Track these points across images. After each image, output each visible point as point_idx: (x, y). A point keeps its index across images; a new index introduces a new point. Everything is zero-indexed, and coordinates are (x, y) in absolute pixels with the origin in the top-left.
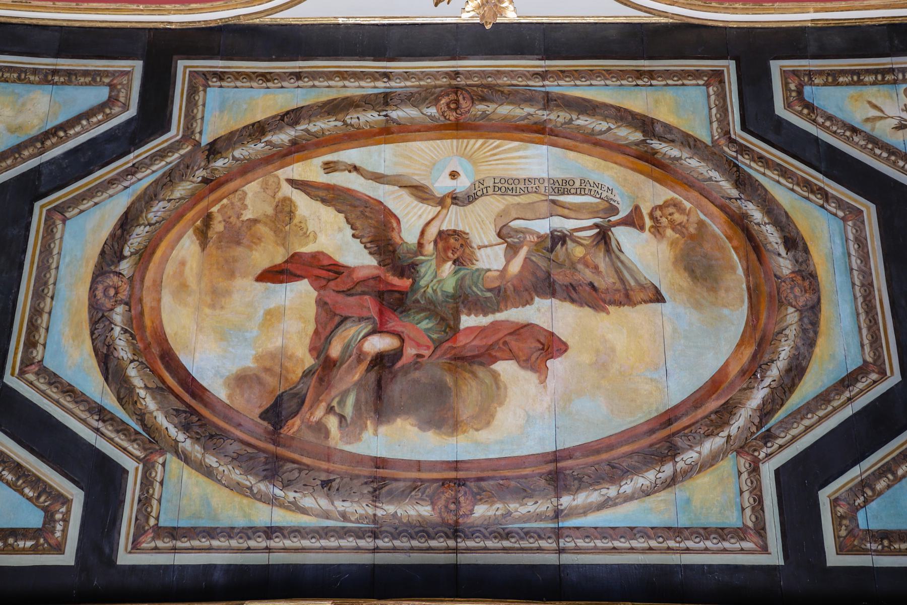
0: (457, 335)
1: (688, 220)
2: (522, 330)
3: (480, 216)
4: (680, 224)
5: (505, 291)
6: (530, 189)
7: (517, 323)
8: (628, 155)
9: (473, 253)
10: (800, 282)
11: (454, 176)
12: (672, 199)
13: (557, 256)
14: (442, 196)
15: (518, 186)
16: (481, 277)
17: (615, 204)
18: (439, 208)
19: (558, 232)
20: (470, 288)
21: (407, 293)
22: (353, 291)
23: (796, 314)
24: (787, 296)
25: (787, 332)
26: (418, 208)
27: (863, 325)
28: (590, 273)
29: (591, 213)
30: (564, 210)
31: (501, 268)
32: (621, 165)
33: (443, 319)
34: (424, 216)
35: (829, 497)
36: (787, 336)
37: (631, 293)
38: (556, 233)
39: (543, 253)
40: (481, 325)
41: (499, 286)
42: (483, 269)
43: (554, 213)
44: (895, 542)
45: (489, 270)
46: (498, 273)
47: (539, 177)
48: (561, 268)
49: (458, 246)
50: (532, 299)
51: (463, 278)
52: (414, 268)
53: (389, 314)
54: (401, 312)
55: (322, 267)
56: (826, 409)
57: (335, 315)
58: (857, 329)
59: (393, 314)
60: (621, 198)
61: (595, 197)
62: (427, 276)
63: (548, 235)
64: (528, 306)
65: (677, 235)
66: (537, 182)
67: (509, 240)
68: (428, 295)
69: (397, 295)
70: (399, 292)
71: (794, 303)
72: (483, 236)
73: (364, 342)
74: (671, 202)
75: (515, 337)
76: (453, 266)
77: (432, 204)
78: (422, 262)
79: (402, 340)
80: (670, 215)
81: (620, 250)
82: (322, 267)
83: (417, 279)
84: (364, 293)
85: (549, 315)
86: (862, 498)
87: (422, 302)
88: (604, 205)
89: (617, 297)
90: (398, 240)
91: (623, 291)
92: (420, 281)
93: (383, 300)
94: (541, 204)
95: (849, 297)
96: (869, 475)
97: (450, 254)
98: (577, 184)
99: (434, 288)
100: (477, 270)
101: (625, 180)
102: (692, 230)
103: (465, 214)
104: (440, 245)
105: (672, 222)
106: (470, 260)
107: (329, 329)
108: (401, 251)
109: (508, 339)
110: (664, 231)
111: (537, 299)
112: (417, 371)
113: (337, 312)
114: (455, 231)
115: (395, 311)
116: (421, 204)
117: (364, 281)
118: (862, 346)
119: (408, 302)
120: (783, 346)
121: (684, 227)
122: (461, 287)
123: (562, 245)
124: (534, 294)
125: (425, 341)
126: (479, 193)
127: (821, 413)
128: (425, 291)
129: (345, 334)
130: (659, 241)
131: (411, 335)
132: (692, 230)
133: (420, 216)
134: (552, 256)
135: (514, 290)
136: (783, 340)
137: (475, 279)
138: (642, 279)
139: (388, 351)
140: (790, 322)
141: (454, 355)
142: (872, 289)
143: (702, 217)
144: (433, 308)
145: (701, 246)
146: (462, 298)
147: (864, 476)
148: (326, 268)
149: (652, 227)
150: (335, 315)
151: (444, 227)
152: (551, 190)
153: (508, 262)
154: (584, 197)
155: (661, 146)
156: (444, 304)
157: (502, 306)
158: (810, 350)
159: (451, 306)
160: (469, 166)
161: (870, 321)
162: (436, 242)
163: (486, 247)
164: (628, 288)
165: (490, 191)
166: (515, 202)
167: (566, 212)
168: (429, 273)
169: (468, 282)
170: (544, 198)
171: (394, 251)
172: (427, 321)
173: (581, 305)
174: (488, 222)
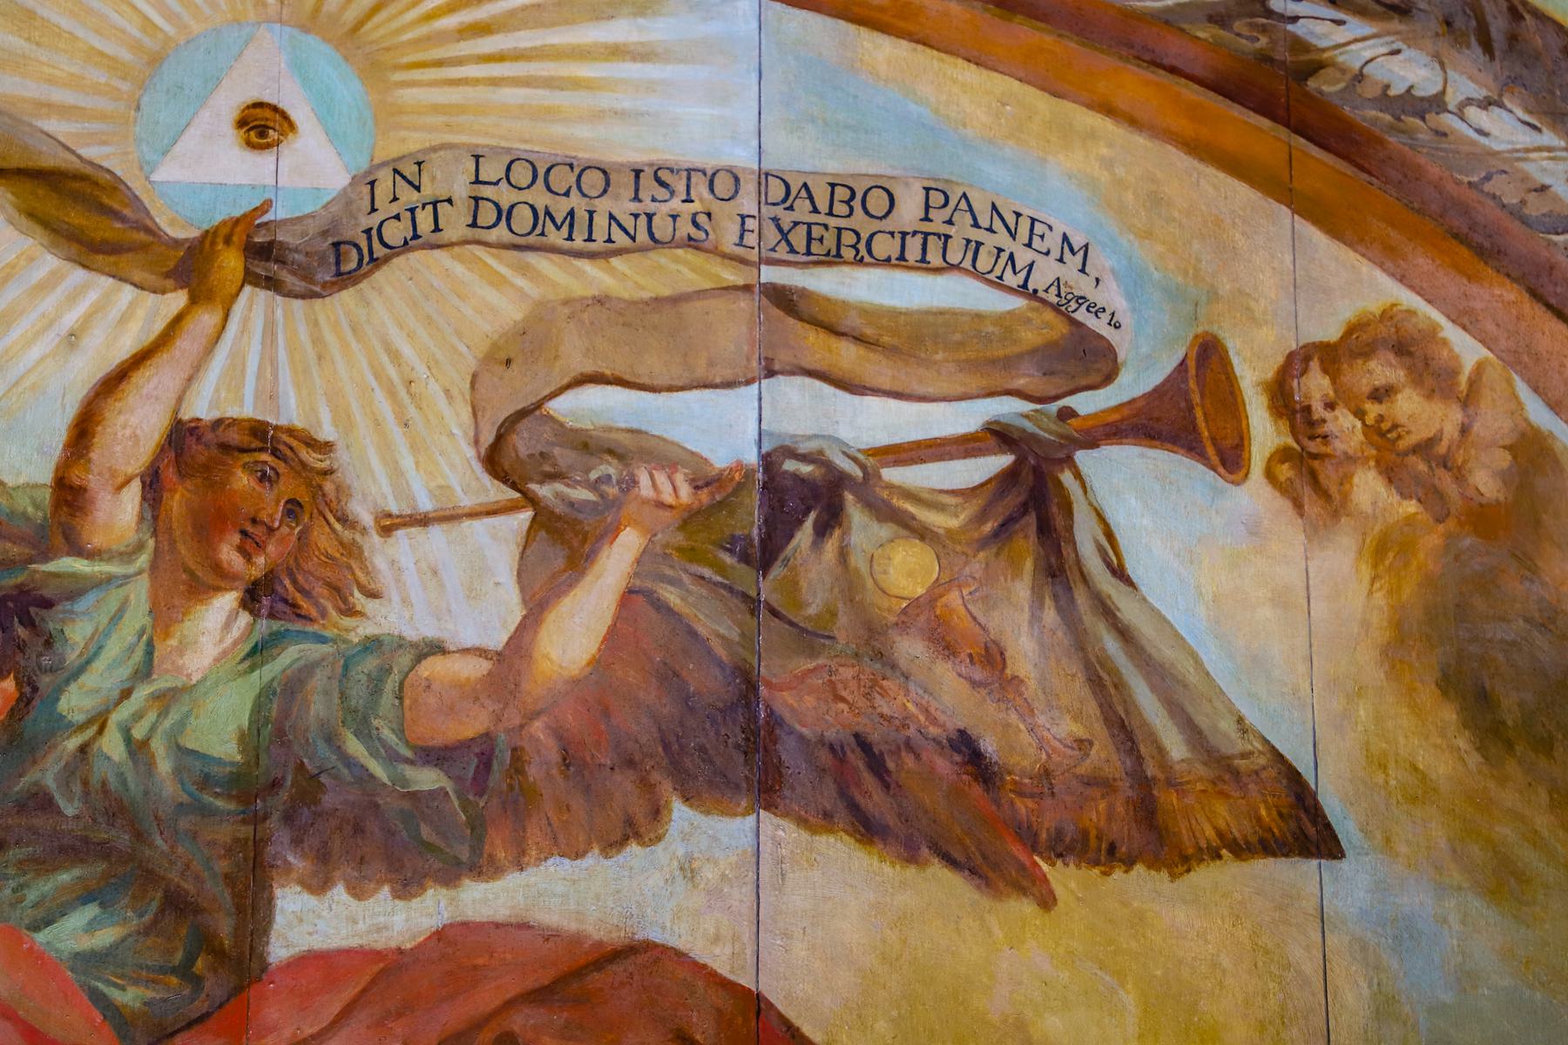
0: (252, 993)
1: (1464, 430)
2: (595, 979)
3: (395, 356)
4: (1425, 448)
5: (518, 760)
6: (662, 228)
7: (576, 940)
8: (1173, 70)
9: (353, 550)
11: (262, 131)
12: (1387, 315)
13: (791, 586)
14: (194, 233)
15: (603, 206)
16: (391, 685)
17: (1099, 325)
18: (177, 300)
19: (804, 458)
20: (331, 739)
26: (59, 293)
28: (963, 686)
29: (973, 366)
30: (834, 342)
31: (497, 639)
32: (1133, 122)
34: (95, 339)
37: (1168, 799)
38: (790, 466)
39: (721, 569)
40: (380, 942)
41: (487, 736)
42: (401, 643)
43: (783, 358)
45: (436, 648)
46: (474, 669)
47: (710, 164)
48: (813, 653)
49: (273, 511)
50: (657, 813)
51: (293, 687)
52: (30, 623)
60: (1130, 297)
61: (999, 284)
62: (99, 665)
63: (749, 474)
64: (634, 848)
65: (1411, 507)
66: (700, 188)
67: (544, 491)
68: (99, 771)
72: (407, 462)
74: (1384, 330)
75: (559, 1018)
76: (244, 618)
77: (138, 276)
78: (77, 589)
80: (1381, 394)
81: (1119, 573)
83: (45, 681)
85: (741, 896)
87: (70, 810)
88: (1043, 329)
89: (1095, 815)
91: (1126, 789)
92: (59, 691)
94: (718, 305)
97: (228, 554)
98: (909, 211)
99: (138, 733)
100: (373, 644)
101: (1155, 200)
102: (1486, 482)
103: (317, 340)
104: (177, 501)
105: (1382, 435)
106: (337, 591)
110: (1346, 479)
111: (680, 813)
114: (258, 430)
116: (79, 275)
121: (1445, 463)
122: (280, 732)
123: (822, 531)
124: (666, 787)
126: (395, 233)
128: (83, 749)
130: (1316, 533)
132: (1486, 482)
133: (73, 338)
135: (566, 761)
137: (358, 693)
138: (1227, 726)
143: (1538, 413)
144: (124, 839)
145: (1528, 565)
146: (284, 795)
149: (1283, 455)
151: (201, 407)
152: (772, 235)
153: (536, 610)
154: (942, 281)
155: (1340, 35)
156: (184, 824)
159: (224, 832)
160: (347, 88)
162: (153, 484)
163: (423, 521)
164: (1151, 770)
165: (455, 223)
166: (579, 290)
167: (846, 355)
168: (113, 649)
169: (318, 706)
170: (732, 276)
172: (92, 910)
174: (435, 389)
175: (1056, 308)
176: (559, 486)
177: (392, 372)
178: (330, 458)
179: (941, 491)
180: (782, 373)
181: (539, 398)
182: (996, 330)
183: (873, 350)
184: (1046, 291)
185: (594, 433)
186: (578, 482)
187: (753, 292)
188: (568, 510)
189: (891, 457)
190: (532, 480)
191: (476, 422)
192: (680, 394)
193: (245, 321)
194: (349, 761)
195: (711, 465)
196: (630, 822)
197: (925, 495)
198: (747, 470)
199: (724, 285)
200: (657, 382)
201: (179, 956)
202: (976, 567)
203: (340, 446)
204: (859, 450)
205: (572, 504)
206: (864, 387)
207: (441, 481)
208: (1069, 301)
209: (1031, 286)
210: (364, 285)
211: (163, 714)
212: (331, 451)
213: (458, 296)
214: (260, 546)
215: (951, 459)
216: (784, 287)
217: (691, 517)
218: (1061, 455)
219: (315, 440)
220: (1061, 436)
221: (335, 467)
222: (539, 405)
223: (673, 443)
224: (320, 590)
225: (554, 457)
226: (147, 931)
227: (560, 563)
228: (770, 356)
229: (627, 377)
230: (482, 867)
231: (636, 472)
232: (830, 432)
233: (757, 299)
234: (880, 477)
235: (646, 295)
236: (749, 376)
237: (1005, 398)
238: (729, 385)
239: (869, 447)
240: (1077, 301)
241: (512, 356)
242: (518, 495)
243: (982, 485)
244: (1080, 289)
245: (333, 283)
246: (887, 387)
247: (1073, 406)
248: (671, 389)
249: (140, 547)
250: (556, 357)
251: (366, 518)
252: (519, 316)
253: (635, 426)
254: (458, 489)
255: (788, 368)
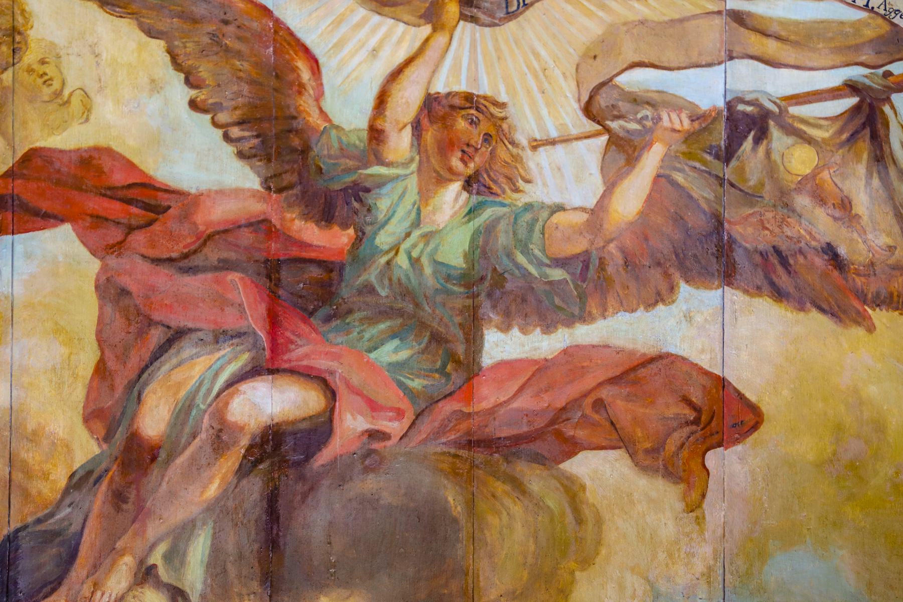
0: (475, 380)
3: (537, 55)
9: (517, 158)
13: (741, 171)
16: (538, 227)
18: (426, 30)
19: (748, 103)
20: (510, 255)
21: (342, 267)
22: (197, 260)
28: (829, 220)
29: (838, 50)
31: (591, 203)
33: (437, 339)
38: (741, 107)
39: (704, 163)
40: (536, 356)
41: (587, 252)
42: (543, 206)
43: (738, 49)
45: (560, 208)
48: (752, 205)
50: (672, 289)
51: (490, 229)
52: (359, 200)
53: (293, 325)
54: (328, 319)
55: (111, 193)
57: (151, 323)
59: (305, 321)
62: (394, 221)
63: (719, 113)
64: (661, 307)
67: (614, 125)
68: (397, 273)
69: (315, 272)
70: (319, 263)
72: (544, 112)
73: (232, 396)
76: (465, 195)
78: (382, 182)
79: (331, 394)
82: (111, 193)
83: (368, 229)
84: (225, 266)
87: (383, 293)
88: (876, 29)
90: (314, 118)
92: (376, 233)
93: (278, 283)
94: (703, 23)
97: (456, 162)
99: (415, 254)
100: (529, 207)
103: (498, 49)
104: (430, 135)
106: (509, 179)
107: (135, 361)
108: (321, 150)
109: (605, 393)
111: (684, 289)
112: (371, 476)
113: (156, 316)
114: (469, 97)
115: (311, 314)
117: (226, 231)
119: (345, 292)
122: (484, 253)
123: (757, 141)
124: (677, 276)
125: (390, 396)
128: (388, 263)
129: (178, 376)
131: (355, 380)
134: (729, 172)
135: (626, 263)
137: (522, 233)
139: (293, 423)
141: (469, 433)
144: (410, 307)
146: (487, 284)
148: (120, 194)
150: (151, 323)
151: (440, 87)
153: (610, 187)
156: (439, 299)
157: (593, 306)
159: (459, 303)
162: (417, 127)
163: (553, 142)
166: (631, 17)
167: (771, 47)
168: (401, 212)
169: (503, 239)
171: (305, 150)
172: (396, 342)
173: (801, 308)
174: (557, 73)
175: (883, 17)
176: (621, 122)
177: (536, 65)
178: (505, 111)
179: (820, 118)
180: (737, 58)
181: (611, 75)
182: (851, 30)
183: (786, 44)
184: (879, 8)
185: (639, 93)
186: (631, 120)
187: (722, 14)
188: (626, 134)
189: (794, 101)
190: (608, 119)
191: (579, 90)
192: (684, 71)
193: (461, 40)
194: (518, 266)
195: (700, 108)
196: (658, 294)
197: (812, 121)
198: (719, 111)
199: (707, 11)
200: (672, 65)
201: (439, 364)
202: (837, 158)
203: (510, 104)
204: (777, 98)
205: (628, 131)
206: (781, 64)
207: (561, 122)
208: (891, 13)
209: (870, 6)
210: (520, 18)
211: (427, 244)
212: (505, 108)
213: (569, 22)
214: (471, 158)
215: (825, 101)
216: (739, 11)
217: (689, 136)
218: (884, 97)
219: (497, 102)
220: (885, 86)
221: (508, 116)
222: (611, 80)
223: (680, 98)
224: (502, 180)
225: (619, 108)
226: (423, 352)
227: (622, 162)
228: (731, 49)
229: (657, 63)
230: (585, 317)
231: (661, 113)
232: (763, 89)
233: (724, 18)
234: (788, 112)
235: (666, 18)
236: (720, 60)
237: (855, 67)
238: (709, 65)
239: (783, 96)
240: (895, 13)
241: (597, 54)
242: (600, 127)
243: (842, 114)
244: (897, 6)
245: (505, 18)
246: (792, 63)
247: (891, 70)
248: (679, 68)
249: (412, 160)
250: (620, 54)
251: (524, 142)
252: (600, 32)
253: (660, 89)
254: (570, 126)
255: (741, 55)
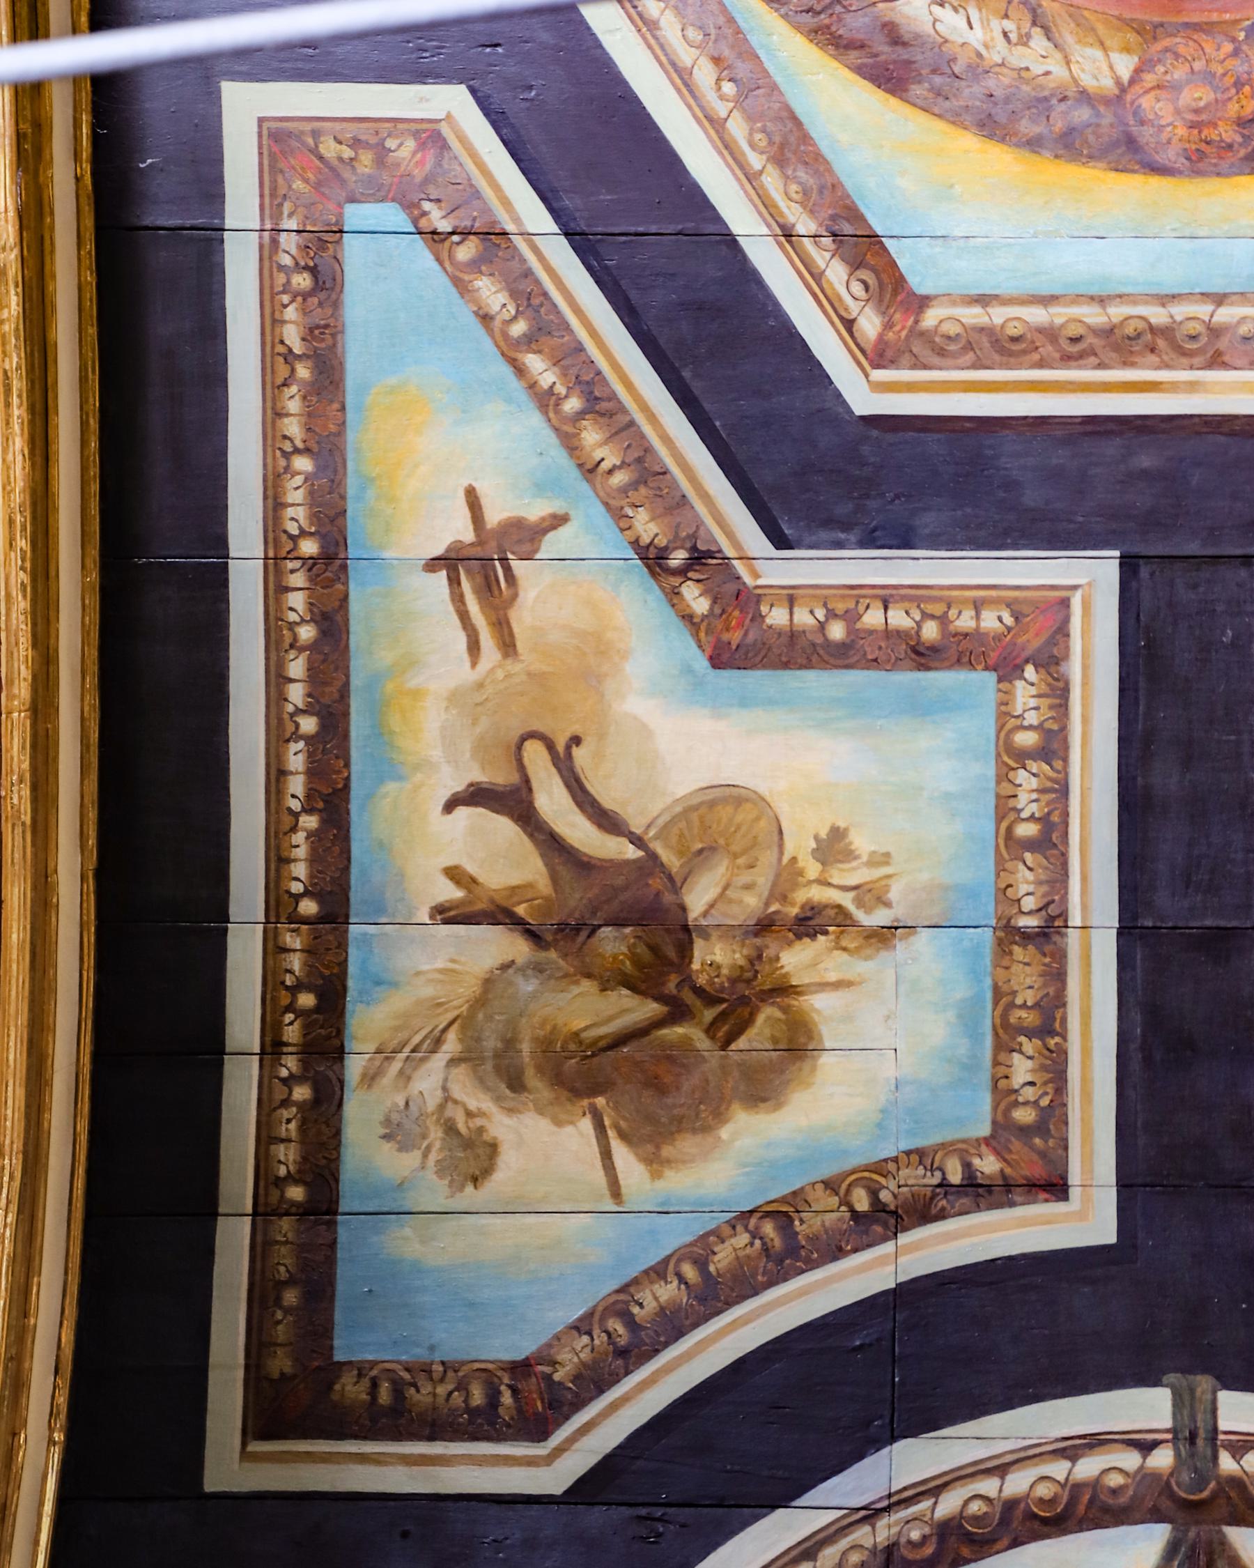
10: (1233, 109)
23: (1107, 83)
24: (1177, 56)
25: (1039, 42)
27: (1058, 315)
35: (449, 116)
36: (1024, 40)
44: (305, 312)
56: (753, 146)
58: (1045, 290)
71: (1149, 79)
86: (444, 226)
95: (1169, 280)
96: (523, 261)
118: (983, 300)
120: (985, 25)
127: (737, 128)
136: (1009, 25)
140: (1075, 57)
142: (1197, 361)
147: (518, 241)
158: (968, 118)
161: (1075, 340)
